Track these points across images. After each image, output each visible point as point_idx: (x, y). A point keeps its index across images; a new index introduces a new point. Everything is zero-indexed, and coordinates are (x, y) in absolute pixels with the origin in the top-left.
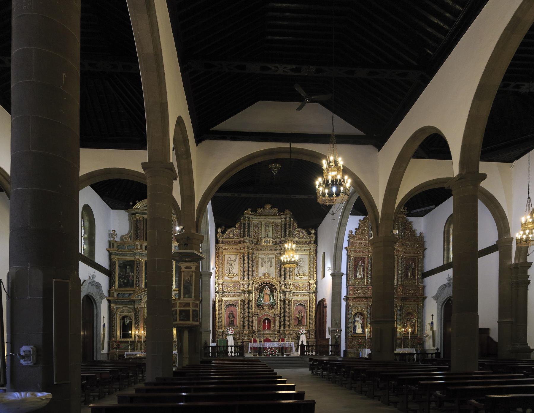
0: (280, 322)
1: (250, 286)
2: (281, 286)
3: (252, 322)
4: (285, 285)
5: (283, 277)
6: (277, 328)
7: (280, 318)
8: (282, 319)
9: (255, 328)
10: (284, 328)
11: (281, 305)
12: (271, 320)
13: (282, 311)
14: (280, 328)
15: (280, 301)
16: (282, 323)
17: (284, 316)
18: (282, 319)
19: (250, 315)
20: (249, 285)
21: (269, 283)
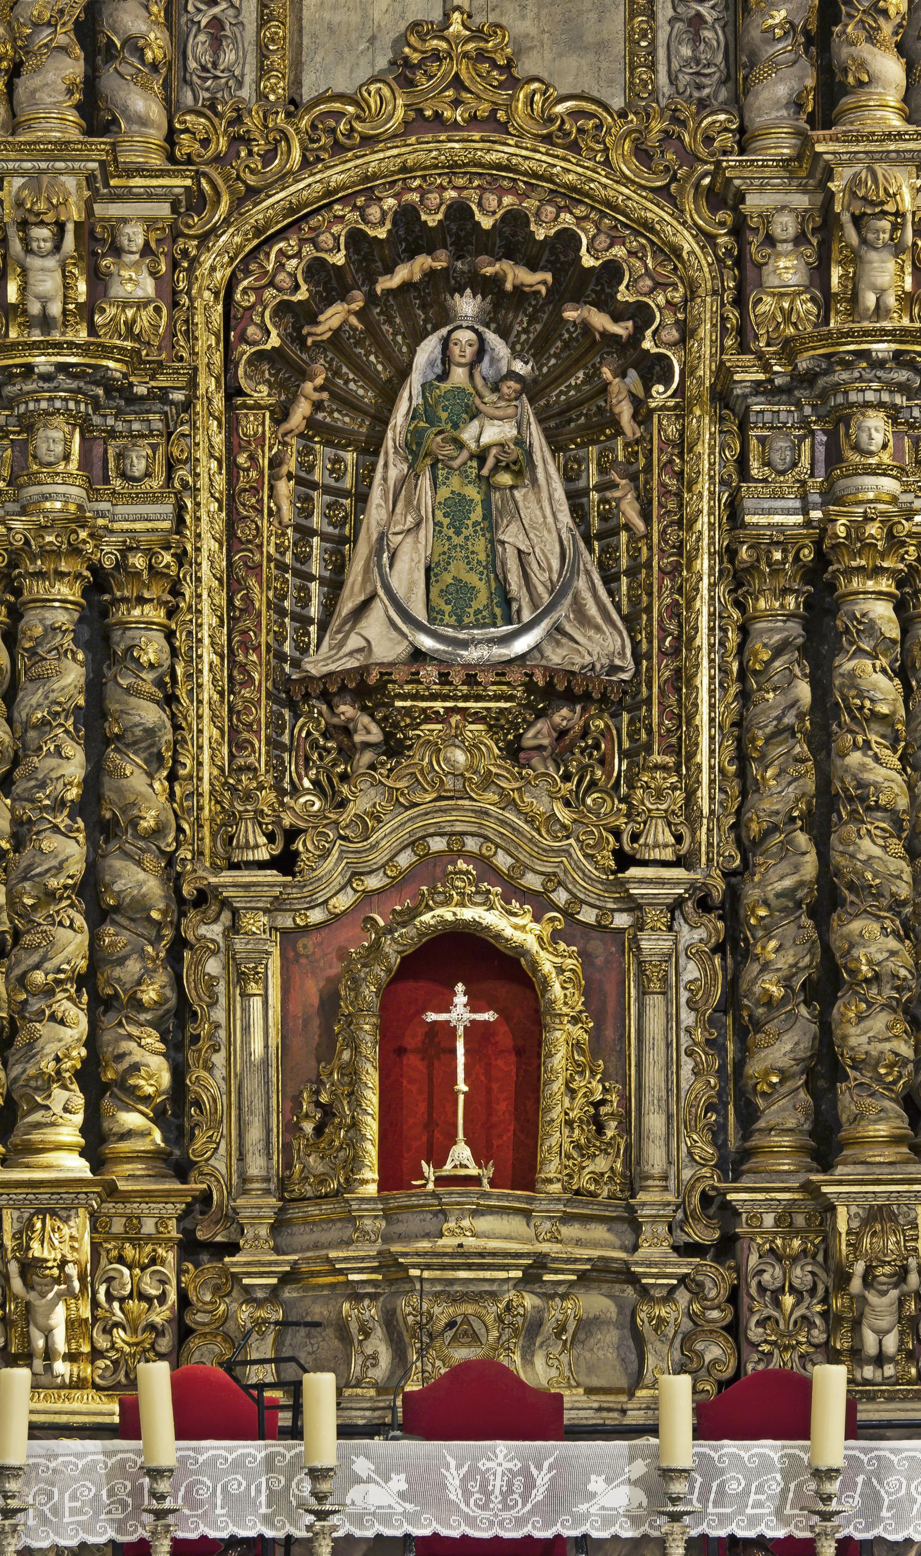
0: (734, 1017)
1: (135, 283)
2: (743, 274)
3: (179, 1027)
4: (822, 234)
5: (779, 90)
6: (673, 1154)
7: (734, 947)
8: (780, 958)
9: (242, 1151)
10: (825, 1144)
11: (745, 683)
12: (555, 969)
13: (783, 790)
14: (734, 1164)
15: (738, 578)
16: (782, 1050)
17: (827, 899)
18: (780, 958)
19: (136, 879)
20: (96, 247)
21: (512, 238)
